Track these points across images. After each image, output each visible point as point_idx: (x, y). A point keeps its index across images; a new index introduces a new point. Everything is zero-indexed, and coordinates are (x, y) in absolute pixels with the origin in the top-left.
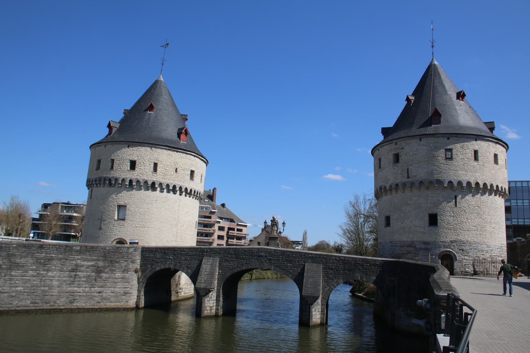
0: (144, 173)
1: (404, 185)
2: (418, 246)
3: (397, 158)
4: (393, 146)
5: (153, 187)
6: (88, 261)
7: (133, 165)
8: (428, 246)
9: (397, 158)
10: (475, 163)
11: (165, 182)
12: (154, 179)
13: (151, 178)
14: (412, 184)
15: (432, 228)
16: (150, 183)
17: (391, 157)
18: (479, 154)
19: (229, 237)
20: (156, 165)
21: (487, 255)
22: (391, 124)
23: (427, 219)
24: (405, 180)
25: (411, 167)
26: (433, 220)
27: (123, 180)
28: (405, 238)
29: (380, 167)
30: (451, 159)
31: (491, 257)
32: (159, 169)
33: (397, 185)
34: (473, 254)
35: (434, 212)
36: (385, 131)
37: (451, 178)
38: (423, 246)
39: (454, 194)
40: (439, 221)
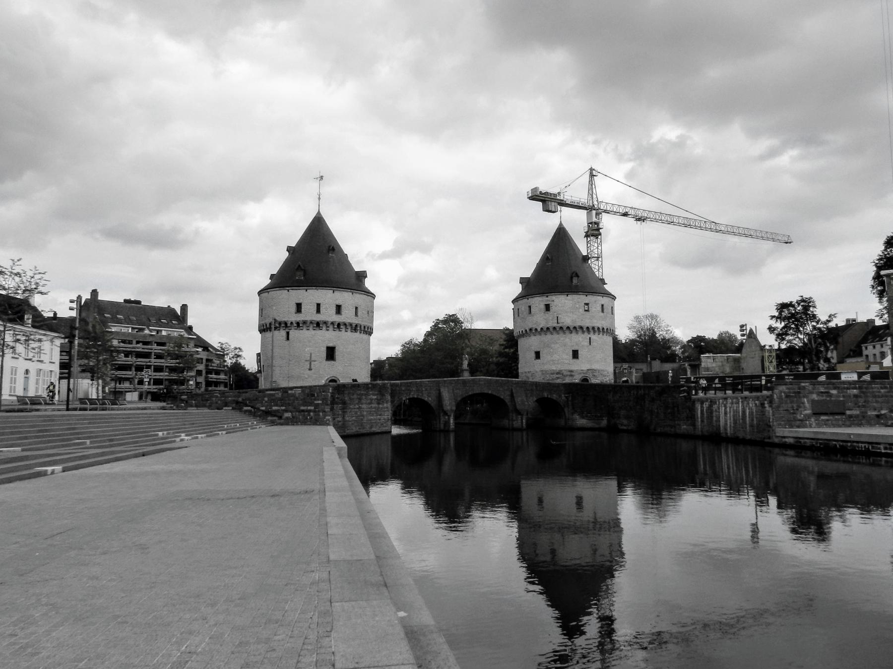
0: (347, 316)
1: (554, 328)
2: (565, 373)
3: (547, 308)
4: (545, 298)
5: (355, 328)
6: (374, 395)
7: (339, 309)
9: (547, 308)
11: (363, 324)
13: (355, 321)
14: (561, 328)
17: (543, 307)
19: (209, 372)
20: (356, 308)
22: (528, 274)
24: (555, 325)
26: (575, 354)
27: (332, 323)
29: (530, 312)
30: (587, 311)
32: (359, 313)
33: (548, 328)
36: (523, 281)
37: (587, 325)
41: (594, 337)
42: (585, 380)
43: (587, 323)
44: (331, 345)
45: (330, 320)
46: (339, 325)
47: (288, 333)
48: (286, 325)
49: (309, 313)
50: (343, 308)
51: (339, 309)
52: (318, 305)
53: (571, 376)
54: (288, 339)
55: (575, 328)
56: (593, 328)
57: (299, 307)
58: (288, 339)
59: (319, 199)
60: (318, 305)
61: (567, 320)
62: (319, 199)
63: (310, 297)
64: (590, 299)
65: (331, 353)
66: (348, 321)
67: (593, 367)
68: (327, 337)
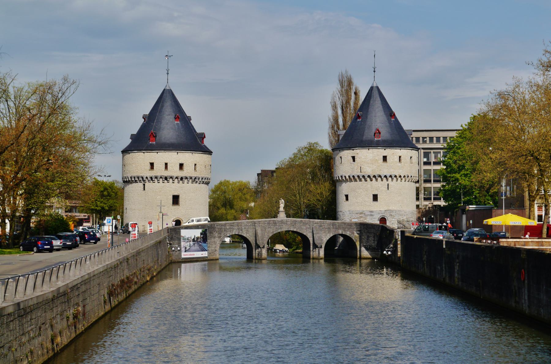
0: (188, 171)
3: (354, 158)
4: (351, 151)
5: (194, 180)
7: (181, 166)
8: (372, 214)
10: (400, 164)
11: (200, 176)
12: (196, 176)
13: (194, 175)
15: (375, 202)
16: (193, 178)
18: (402, 158)
20: (195, 165)
21: (405, 218)
23: (372, 197)
24: (359, 174)
25: (362, 167)
26: (375, 198)
27: (177, 178)
28: (359, 209)
31: (407, 218)
32: (197, 169)
34: (398, 217)
35: (376, 193)
38: (369, 213)
39: (387, 182)
40: (378, 199)
41: (393, 183)
42: (383, 220)
43: (385, 170)
44: (176, 194)
45: (175, 175)
46: (182, 179)
47: (144, 185)
48: (141, 179)
49: (159, 170)
50: (184, 165)
51: (181, 166)
52: (166, 164)
53: (371, 215)
54: (144, 189)
55: (374, 176)
56: (391, 176)
57: (152, 165)
58: (144, 189)
59: (168, 74)
60: (166, 164)
61: (368, 170)
62: (168, 74)
63: (160, 158)
64: (388, 152)
65: (176, 200)
66: (188, 175)
67: (391, 208)
68: (174, 188)
